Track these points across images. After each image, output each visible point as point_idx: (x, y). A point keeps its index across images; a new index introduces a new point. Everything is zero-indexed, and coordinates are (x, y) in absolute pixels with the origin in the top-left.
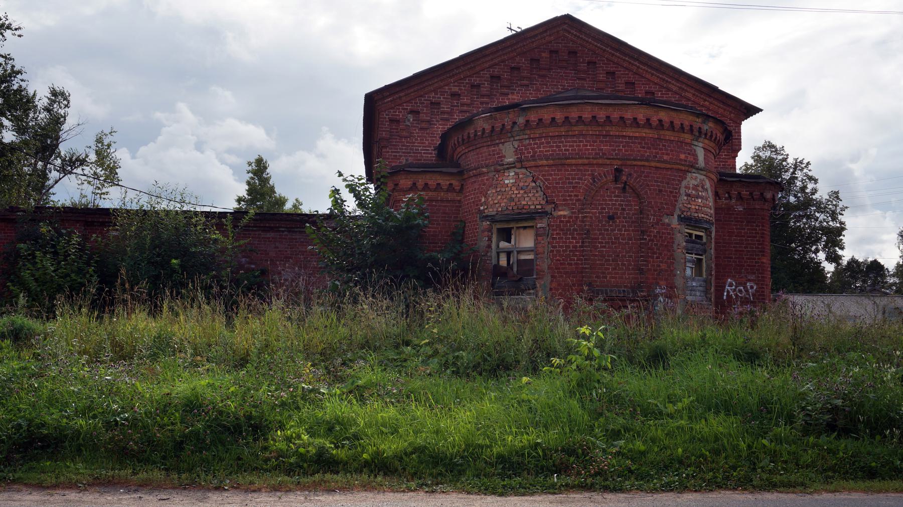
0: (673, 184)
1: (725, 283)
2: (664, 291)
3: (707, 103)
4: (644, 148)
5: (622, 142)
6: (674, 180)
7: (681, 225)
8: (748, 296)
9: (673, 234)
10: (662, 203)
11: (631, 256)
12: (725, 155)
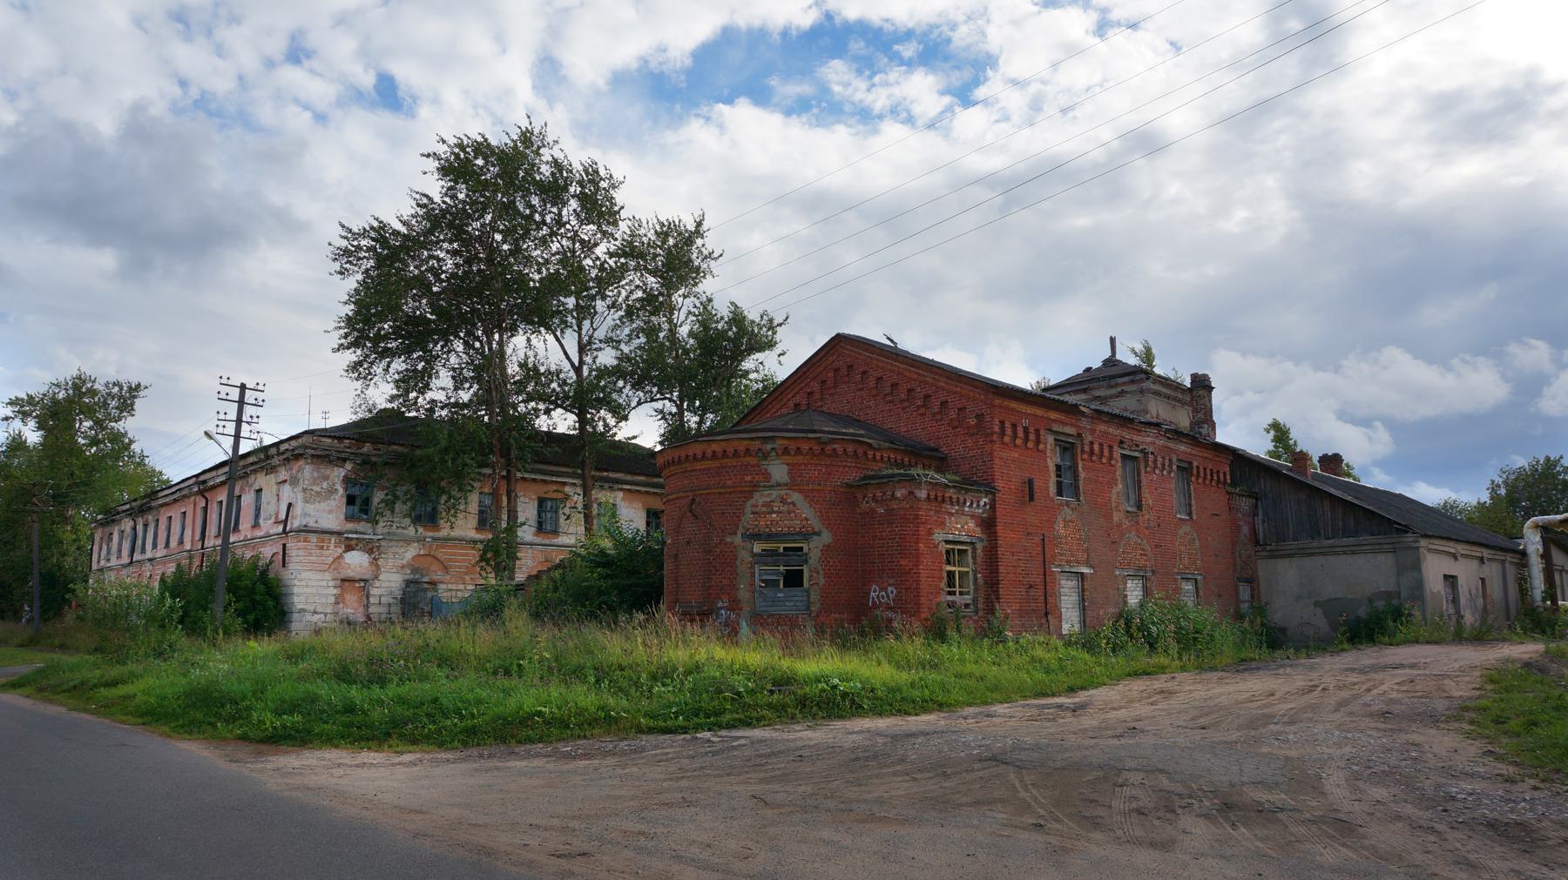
1: (870, 589)
2: (725, 605)
3: (958, 389)
6: (737, 501)
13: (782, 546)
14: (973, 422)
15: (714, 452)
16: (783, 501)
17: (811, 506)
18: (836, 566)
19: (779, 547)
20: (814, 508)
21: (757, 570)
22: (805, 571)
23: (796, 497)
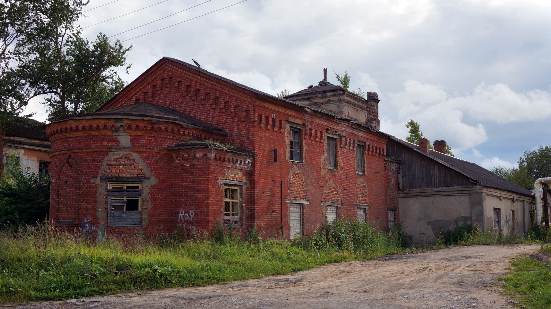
0: (97, 160)
1: (179, 212)
2: (89, 221)
3: (235, 95)
4: (80, 142)
5: (71, 141)
6: (98, 157)
7: (103, 182)
8: (190, 219)
9: (96, 188)
10: (89, 172)
11: (73, 202)
12: (248, 126)
13: (126, 185)
14: (243, 114)
15: (84, 126)
16: (127, 158)
17: (144, 162)
18: (159, 198)
19: (124, 186)
20: (146, 163)
21: (109, 200)
22: (139, 201)
23: (135, 155)
